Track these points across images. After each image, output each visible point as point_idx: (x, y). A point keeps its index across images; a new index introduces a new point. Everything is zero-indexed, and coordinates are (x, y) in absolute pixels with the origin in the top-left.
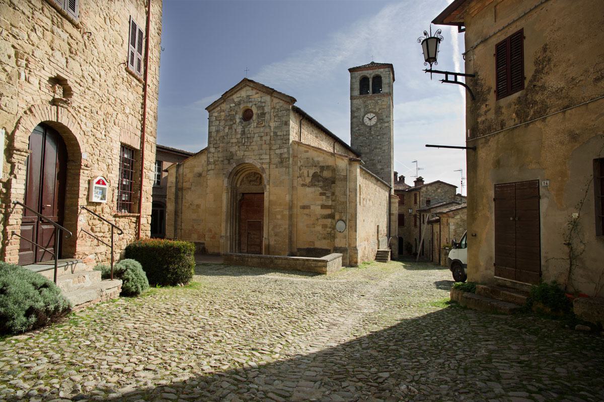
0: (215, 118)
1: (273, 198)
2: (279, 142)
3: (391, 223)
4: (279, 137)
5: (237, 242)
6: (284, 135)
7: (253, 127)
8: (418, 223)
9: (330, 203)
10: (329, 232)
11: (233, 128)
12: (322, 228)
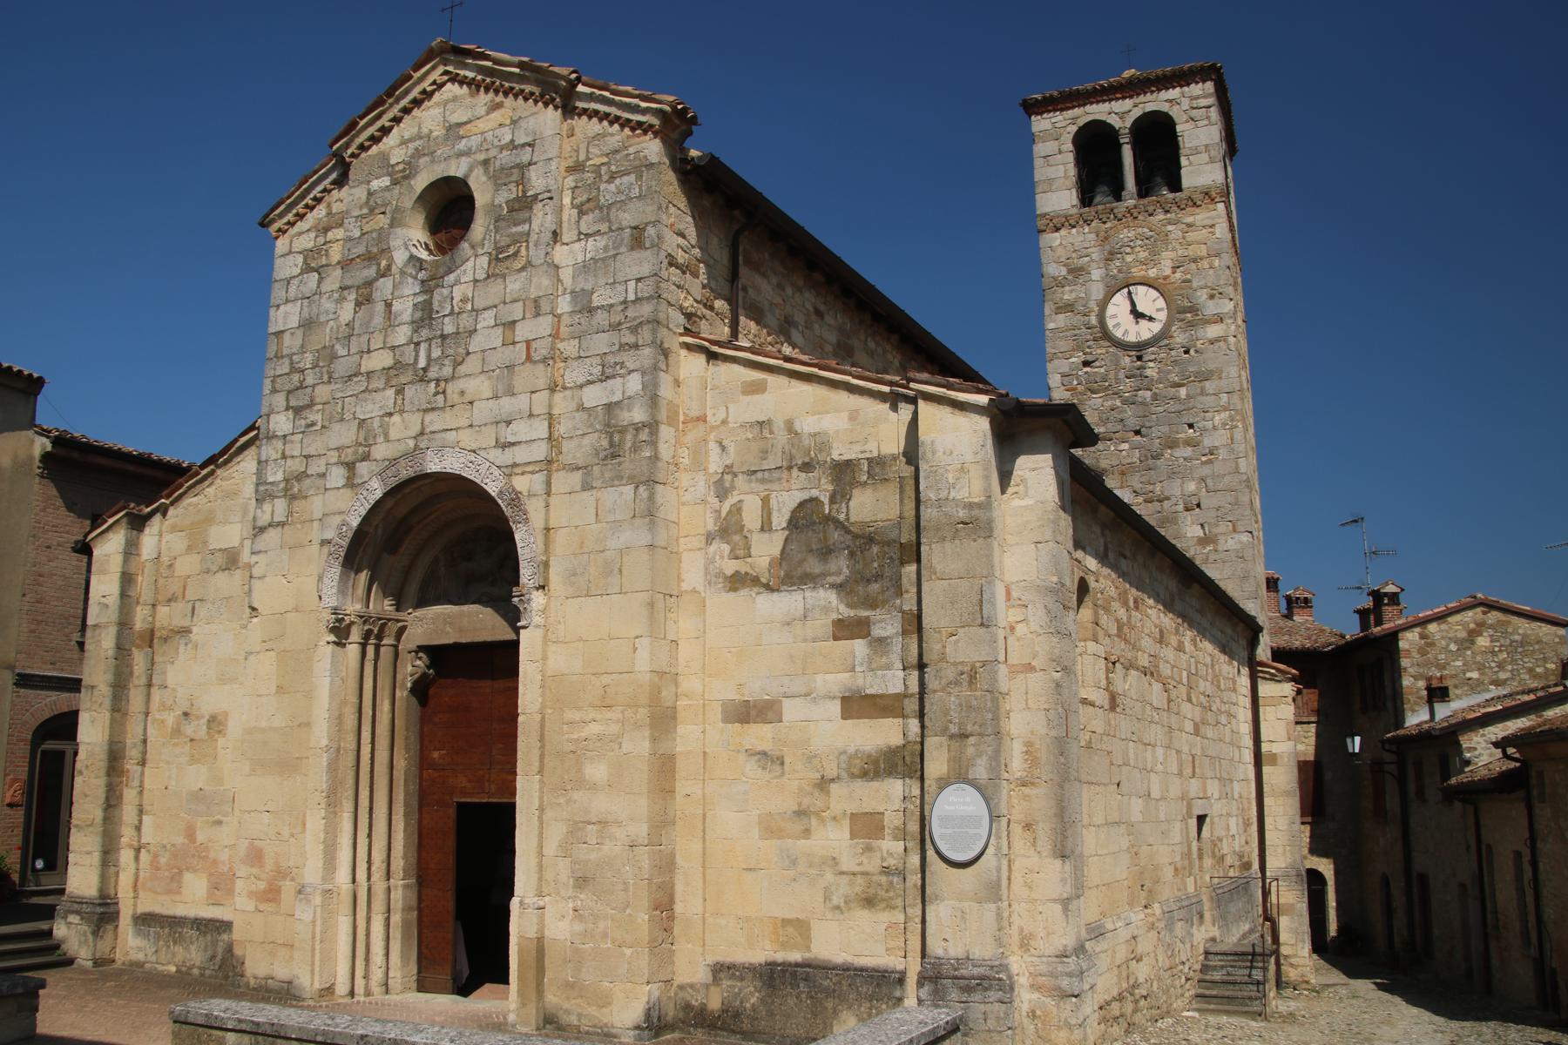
0: (300, 259)
1: (559, 661)
2: (601, 343)
3: (1267, 801)
4: (601, 318)
5: (396, 918)
6: (625, 302)
7: (469, 277)
8: (1392, 803)
9: (894, 680)
10: (891, 862)
11: (377, 295)
12: (853, 836)
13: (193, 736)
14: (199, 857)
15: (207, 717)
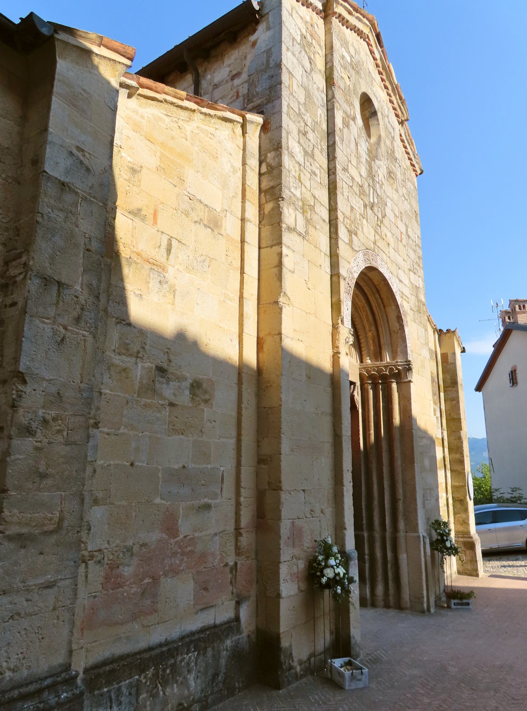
13: (172, 399)
14: (183, 554)
15: (190, 381)
